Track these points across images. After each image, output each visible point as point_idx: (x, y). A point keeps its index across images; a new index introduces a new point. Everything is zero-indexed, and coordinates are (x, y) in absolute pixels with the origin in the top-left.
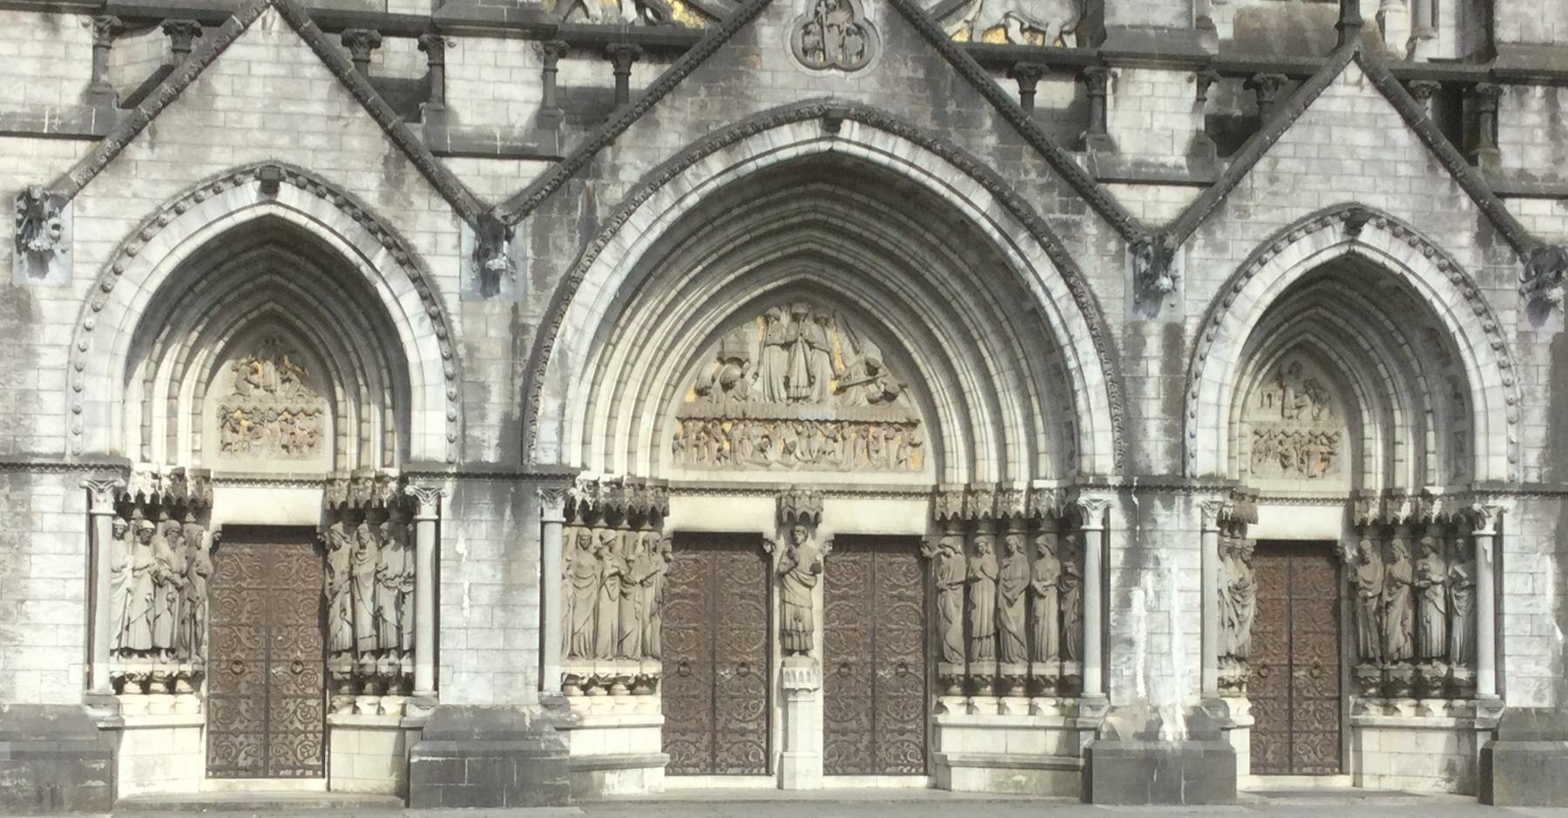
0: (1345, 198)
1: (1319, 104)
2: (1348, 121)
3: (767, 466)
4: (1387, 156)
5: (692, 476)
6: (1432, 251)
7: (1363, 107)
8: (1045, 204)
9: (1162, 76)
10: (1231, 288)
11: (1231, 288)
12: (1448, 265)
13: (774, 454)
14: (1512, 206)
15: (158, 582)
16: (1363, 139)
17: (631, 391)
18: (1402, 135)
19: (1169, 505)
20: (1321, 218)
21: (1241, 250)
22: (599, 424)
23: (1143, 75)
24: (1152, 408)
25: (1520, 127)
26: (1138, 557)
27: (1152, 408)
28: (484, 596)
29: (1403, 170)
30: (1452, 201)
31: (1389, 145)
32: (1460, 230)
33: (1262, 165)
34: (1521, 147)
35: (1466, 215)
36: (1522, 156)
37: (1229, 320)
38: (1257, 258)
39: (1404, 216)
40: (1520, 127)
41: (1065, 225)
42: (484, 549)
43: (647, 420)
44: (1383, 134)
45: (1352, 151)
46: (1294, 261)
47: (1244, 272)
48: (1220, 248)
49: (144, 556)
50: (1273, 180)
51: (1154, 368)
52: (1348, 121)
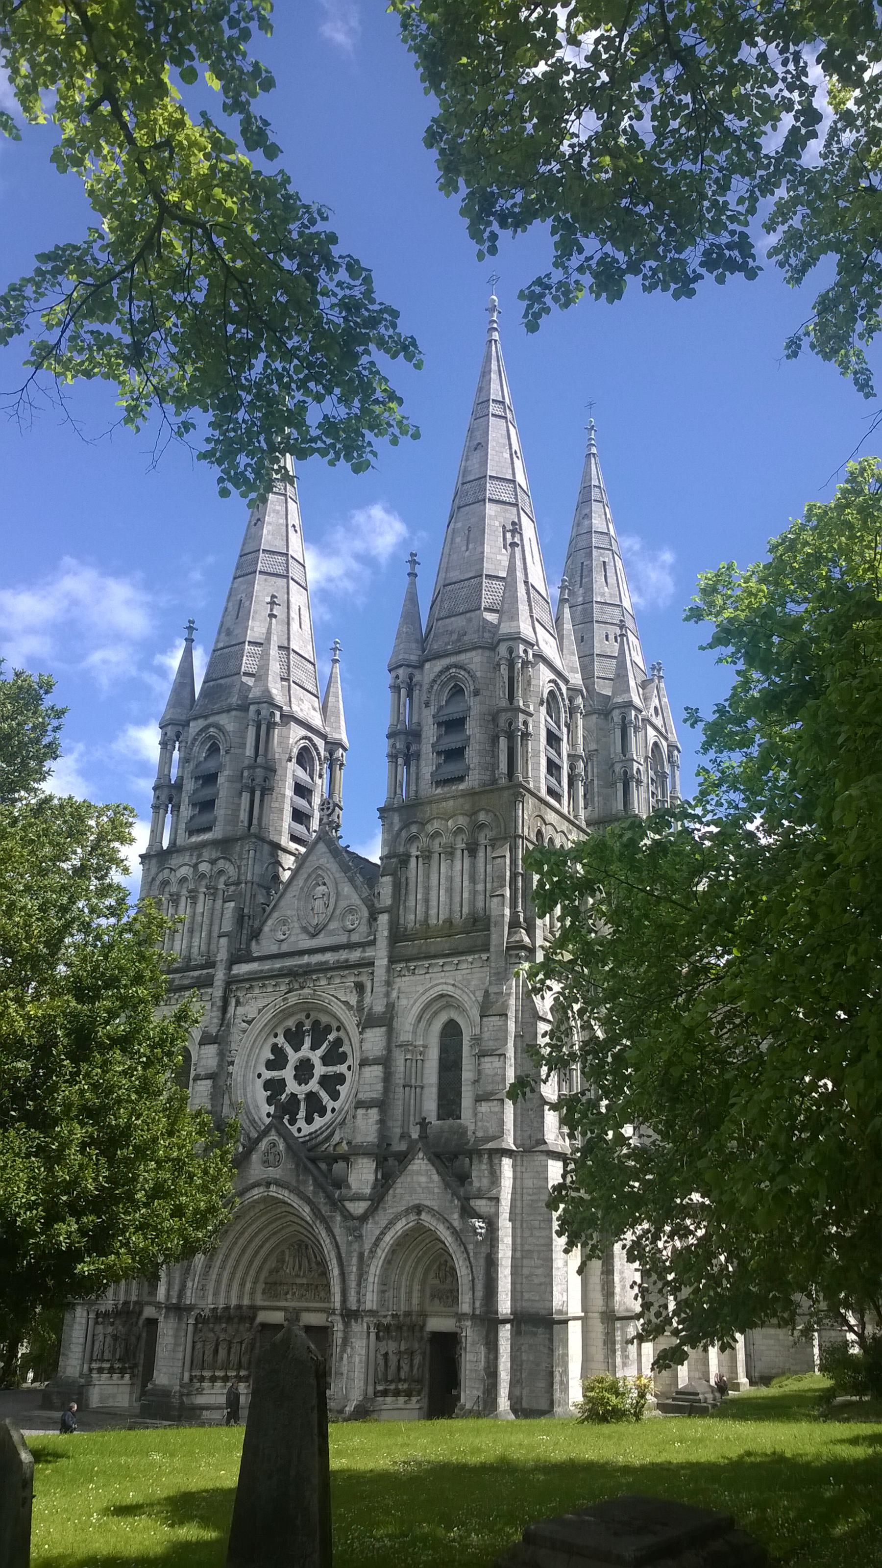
0: (417, 1202)
1: (410, 1167)
2: (418, 1173)
3: (286, 1300)
4: (431, 1185)
5: (266, 1303)
6: (445, 1221)
7: (424, 1167)
8: (325, 1210)
9: (365, 1160)
10: (378, 1240)
11: (378, 1240)
12: (450, 1227)
13: (289, 1296)
14: (472, 1203)
15: (115, 1338)
16: (423, 1179)
17: (239, 1275)
18: (436, 1177)
19: (356, 1322)
20: (407, 1212)
21: (383, 1223)
22: (223, 1287)
23: (360, 1161)
24: (353, 1284)
25: (479, 1170)
26: (346, 1341)
27: (353, 1284)
28: (169, 1347)
29: (436, 1190)
30: (452, 1201)
31: (432, 1181)
32: (453, 1213)
33: (391, 1192)
34: (480, 1178)
35: (456, 1207)
36: (480, 1181)
37: (379, 1251)
38: (387, 1228)
39: (436, 1208)
40: (479, 1170)
41: (331, 1217)
42: (171, 1332)
43: (248, 1285)
44: (430, 1177)
45: (419, 1183)
46: (400, 1226)
47: (383, 1233)
48: (376, 1223)
49: (110, 1329)
50: (394, 1197)
51: (354, 1269)
52: (418, 1173)
